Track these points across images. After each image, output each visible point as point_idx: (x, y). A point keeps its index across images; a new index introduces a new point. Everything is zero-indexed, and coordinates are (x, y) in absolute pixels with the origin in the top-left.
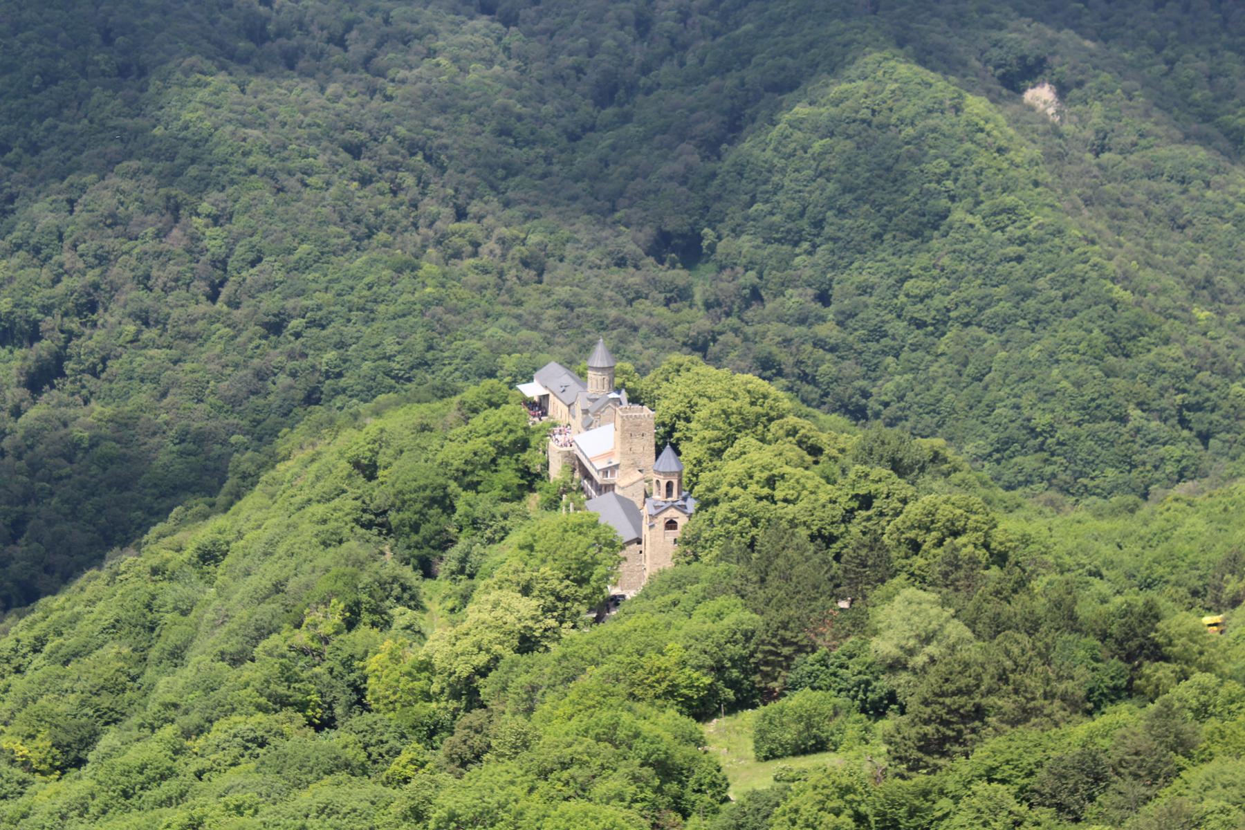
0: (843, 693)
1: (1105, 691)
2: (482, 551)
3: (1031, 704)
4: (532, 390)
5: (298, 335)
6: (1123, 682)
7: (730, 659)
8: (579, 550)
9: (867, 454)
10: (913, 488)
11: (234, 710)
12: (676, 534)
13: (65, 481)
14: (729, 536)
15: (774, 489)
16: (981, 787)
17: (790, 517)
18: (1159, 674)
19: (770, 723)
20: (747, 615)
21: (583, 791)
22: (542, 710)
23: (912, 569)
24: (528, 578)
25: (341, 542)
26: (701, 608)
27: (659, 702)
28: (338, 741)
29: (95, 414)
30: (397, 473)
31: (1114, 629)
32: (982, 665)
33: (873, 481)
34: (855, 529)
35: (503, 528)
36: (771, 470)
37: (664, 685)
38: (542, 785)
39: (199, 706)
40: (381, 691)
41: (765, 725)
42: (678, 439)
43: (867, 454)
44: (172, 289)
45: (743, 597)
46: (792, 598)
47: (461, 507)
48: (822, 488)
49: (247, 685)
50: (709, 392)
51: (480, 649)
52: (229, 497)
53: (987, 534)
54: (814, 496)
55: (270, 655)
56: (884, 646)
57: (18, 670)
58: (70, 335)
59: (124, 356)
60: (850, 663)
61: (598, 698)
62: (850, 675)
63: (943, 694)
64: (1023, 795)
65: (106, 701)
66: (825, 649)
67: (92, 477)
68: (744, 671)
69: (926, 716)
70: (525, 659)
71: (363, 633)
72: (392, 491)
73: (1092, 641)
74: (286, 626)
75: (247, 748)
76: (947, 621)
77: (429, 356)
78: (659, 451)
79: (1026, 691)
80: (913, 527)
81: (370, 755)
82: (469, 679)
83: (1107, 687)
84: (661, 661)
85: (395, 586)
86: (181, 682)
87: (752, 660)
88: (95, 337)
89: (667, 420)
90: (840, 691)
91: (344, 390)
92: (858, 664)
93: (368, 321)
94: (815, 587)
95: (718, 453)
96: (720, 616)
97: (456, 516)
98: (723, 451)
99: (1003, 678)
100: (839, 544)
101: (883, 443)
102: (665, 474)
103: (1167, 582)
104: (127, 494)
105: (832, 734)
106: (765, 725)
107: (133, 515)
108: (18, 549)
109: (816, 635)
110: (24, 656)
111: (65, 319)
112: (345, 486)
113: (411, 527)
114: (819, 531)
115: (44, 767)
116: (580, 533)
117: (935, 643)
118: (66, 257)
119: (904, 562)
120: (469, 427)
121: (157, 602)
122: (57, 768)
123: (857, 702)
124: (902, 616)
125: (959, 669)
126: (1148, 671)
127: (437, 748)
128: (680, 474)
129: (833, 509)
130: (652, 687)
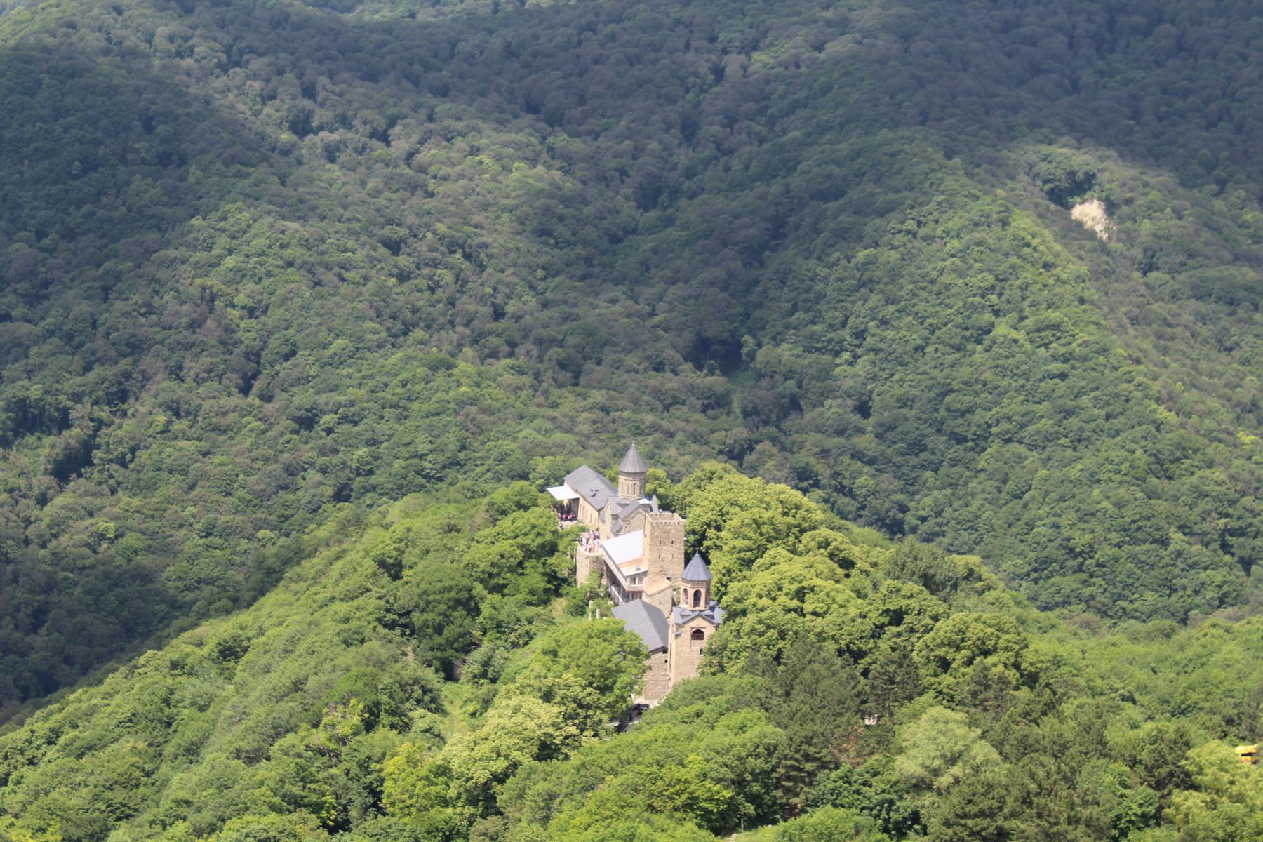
0: (866, 812)
2: (506, 655)
3: (1054, 830)
4: (562, 493)
5: (329, 431)
6: (1151, 810)
8: (603, 657)
9: (899, 569)
10: (945, 605)
11: (247, 809)
12: (703, 644)
13: (88, 571)
14: (755, 648)
15: (803, 602)
17: (818, 630)
18: (1189, 803)
20: (770, 728)
22: (559, 818)
23: (940, 687)
25: (362, 641)
26: (724, 721)
27: (678, 815)
29: (121, 505)
31: (1144, 756)
33: (904, 597)
34: (884, 645)
35: (527, 632)
36: (801, 582)
37: (684, 797)
39: (211, 804)
40: (397, 796)
42: (708, 548)
43: (899, 569)
44: (204, 380)
45: (767, 710)
46: (816, 713)
47: (486, 609)
48: (853, 602)
49: (261, 784)
50: (741, 500)
51: (499, 755)
52: (252, 593)
54: (844, 608)
55: (287, 754)
56: (909, 765)
57: (31, 762)
58: (100, 424)
59: (154, 446)
60: (874, 781)
61: (615, 808)
62: (874, 794)
63: (965, 816)
65: (119, 796)
67: (117, 567)
68: (765, 786)
70: (542, 766)
71: (382, 735)
72: (417, 591)
73: (1121, 767)
74: (304, 725)
76: (974, 741)
77: (462, 455)
78: (688, 559)
79: (1049, 815)
80: (942, 644)
82: (487, 786)
83: (1135, 814)
84: (681, 773)
85: (416, 688)
86: (195, 779)
87: (774, 775)
88: (125, 426)
89: (698, 528)
90: (863, 809)
91: (374, 488)
92: (882, 782)
93: (400, 419)
94: (841, 702)
95: (748, 563)
96: (742, 728)
97: (480, 619)
98: (753, 561)
99: (1026, 801)
100: (867, 660)
101: (915, 558)
102: (693, 582)
103: (1201, 709)
104: (151, 586)
108: (38, 638)
109: (840, 751)
110: (38, 748)
112: (369, 585)
113: (434, 628)
114: (847, 645)
117: (960, 764)
118: (99, 344)
119: (932, 679)
121: (176, 697)
123: (880, 822)
125: (983, 791)
126: (1177, 800)
128: (708, 583)
129: (862, 623)
130: (671, 799)
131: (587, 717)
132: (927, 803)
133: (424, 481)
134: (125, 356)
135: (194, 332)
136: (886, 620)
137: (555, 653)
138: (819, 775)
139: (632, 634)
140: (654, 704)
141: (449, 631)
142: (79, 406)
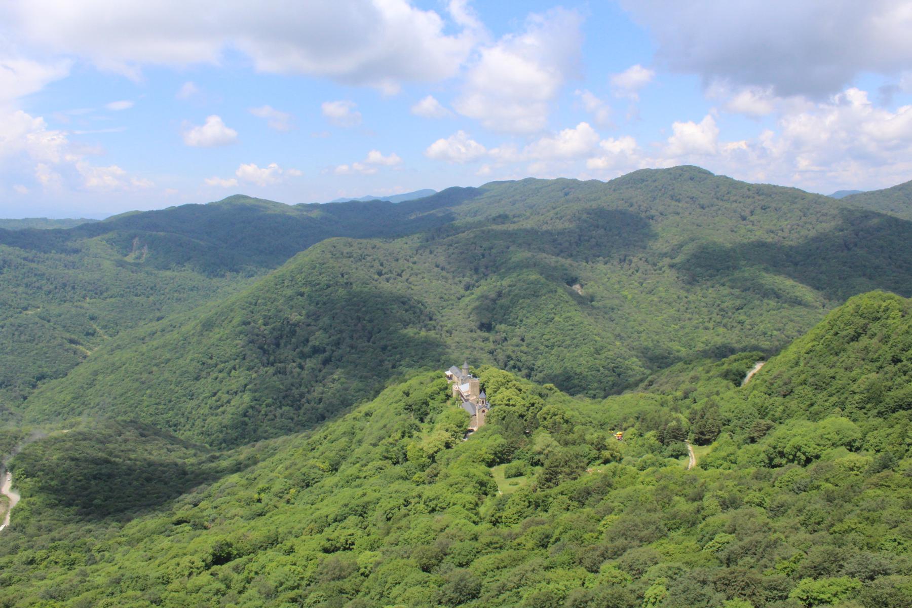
4: (448, 373)
9: (533, 393)
16: (560, 496)
21: (461, 491)
22: (451, 464)
28: (399, 469)
30: (415, 396)
38: (451, 489)
43: (533, 393)
56: (537, 448)
58: (333, 351)
62: (528, 456)
64: (571, 499)
65: (342, 453)
71: (406, 439)
99: (566, 462)
118: (332, 331)
124: (542, 440)
140: (475, 429)
141: (422, 410)
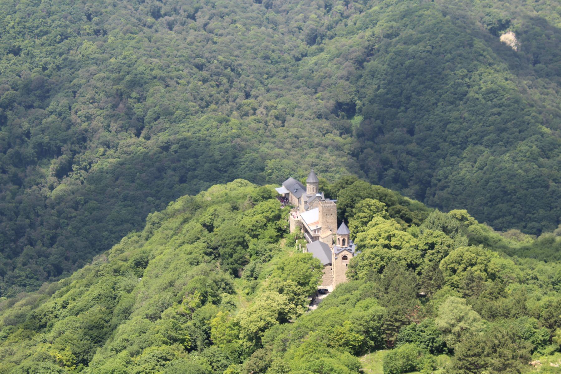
0: (423, 343)
1: (540, 342)
2: (261, 266)
3: (508, 362)
7: (372, 328)
8: (304, 270)
10: (453, 240)
11: (152, 343)
12: (347, 262)
13: (74, 219)
15: (390, 241)
17: (398, 256)
19: (391, 359)
20: (380, 308)
22: (290, 351)
23: (453, 281)
24: (282, 285)
26: (359, 304)
27: (341, 348)
29: (86, 188)
31: (544, 314)
32: (485, 342)
33: (435, 237)
34: (426, 260)
35: (270, 255)
37: (343, 340)
39: (137, 341)
41: (388, 360)
42: (347, 216)
44: (120, 131)
45: (378, 298)
47: (251, 246)
48: (412, 240)
49: (158, 332)
50: (361, 194)
51: (261, 319)
52: (147, 233)
53: (486, 265)
56: (441, 323)
57: (56, 317)
58: (75, 153)
59: (99, 162)
60: (425, 330)
61: (314, 348)
62: (425, 336)
63: (468, 356)
66: (414, 323)
67: (85, 217)
68: (379, 333)
69: (460, 366)
70: (282, 326)
71: (209, 307)
72: (220, 239)
74: (175, 303)
75: (158, 361)
76: (469, 310)
77: (234, 161)
78: (339, 225)
79: (504, 356)
80: (452, 262)
81: (213, 367)
82: (256, 333)
83: (541, 340)
85: (223, 283)
86: (129, 328)
87: (382, 328)
89: (342, 207)
90: (421, 342)
91: (196, 177)
92: (430, 330)
94: (409, 294)
95: (365, 223)
96: (367, 307)
97: (248, 250)
98: (368, 222)
99: (494, 349)
101: (439, 219)
102: (342, 235)
104: (101, 224)
105: (418, 364)
106: (388, 360)
107: (104, 233)
108: (53, 249)
109: (410, 316)
110: (58, 310)
111: (73, 145)
112: (199, 236)
113: (229, 255)
114: (411, 262)
115: (68, 363)
116: (304, 263)
117: (463, 321)
119: (449, 278)
120: (254, 209)
121: (117, 286)
122: (74, 364)
123: (429, 347)
124: (449, 309)
125: (474, 345)
127: (241, 363)
128: (348, 235)
129: (417, 252)
131: (298, 299)
132: (449, 339)
133: (218, 173)
134: (84, 122)
135: (114, 110)
136: (427, 247)
137: (283, 269)
138: (402, 328)
139: (316, 259)
142: (65, 145)
